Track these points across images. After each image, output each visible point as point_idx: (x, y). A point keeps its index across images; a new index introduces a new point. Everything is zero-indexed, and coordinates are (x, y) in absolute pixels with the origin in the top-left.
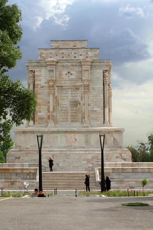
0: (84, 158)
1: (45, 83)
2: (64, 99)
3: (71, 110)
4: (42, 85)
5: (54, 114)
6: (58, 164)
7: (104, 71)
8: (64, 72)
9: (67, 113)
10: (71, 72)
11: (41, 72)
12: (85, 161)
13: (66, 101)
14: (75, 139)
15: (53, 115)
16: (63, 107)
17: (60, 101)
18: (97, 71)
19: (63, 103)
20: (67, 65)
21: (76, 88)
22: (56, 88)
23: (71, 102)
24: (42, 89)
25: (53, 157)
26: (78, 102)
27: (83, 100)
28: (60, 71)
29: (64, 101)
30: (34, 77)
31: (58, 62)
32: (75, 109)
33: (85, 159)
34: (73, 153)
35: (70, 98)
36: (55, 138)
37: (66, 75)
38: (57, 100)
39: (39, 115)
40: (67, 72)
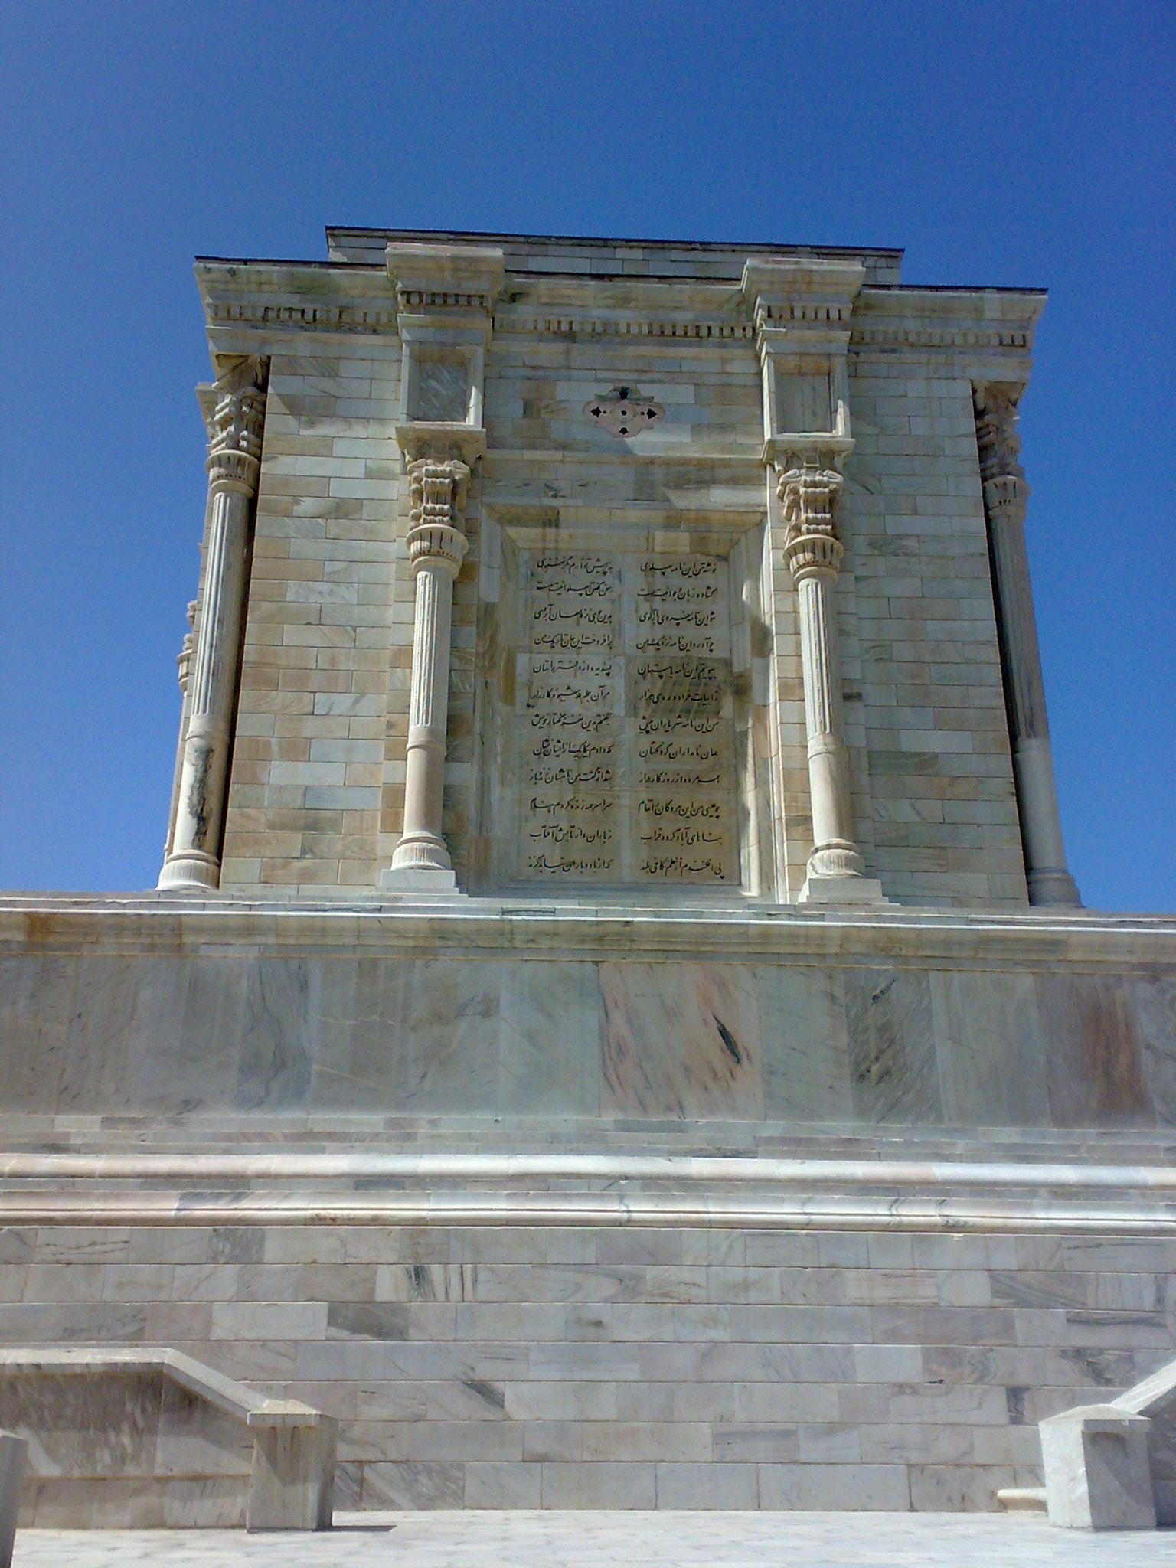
0: (882, 1294)
2: (570, 644)
3: (645, 742)
4: (336, 489)
5: (465, 774)
6: (484, 1391)
7: (980, 395)
8: (578, 393)
10: (645, 390)
11: (332, 374)
12: (894, 1336)
13: (593, 657)
14: (724, 1034)
15: (448, 790)
16: (561, 719)
18: (916, 387)
19: (557, 681)
20: (604, 334)
25: (419, 1274)
26: (720, 675)
28: (540, 373)
29: (567, 656)
30: (262, 427)
31: (514, 298)
32: (685, 739)
33: (894, 1308)
34: (715, 1210)
35: (635, 633)
36: (460, 1014)
37: (596, 412)
38: (493, 638)
39: (281, 789)
40: (606, 389)
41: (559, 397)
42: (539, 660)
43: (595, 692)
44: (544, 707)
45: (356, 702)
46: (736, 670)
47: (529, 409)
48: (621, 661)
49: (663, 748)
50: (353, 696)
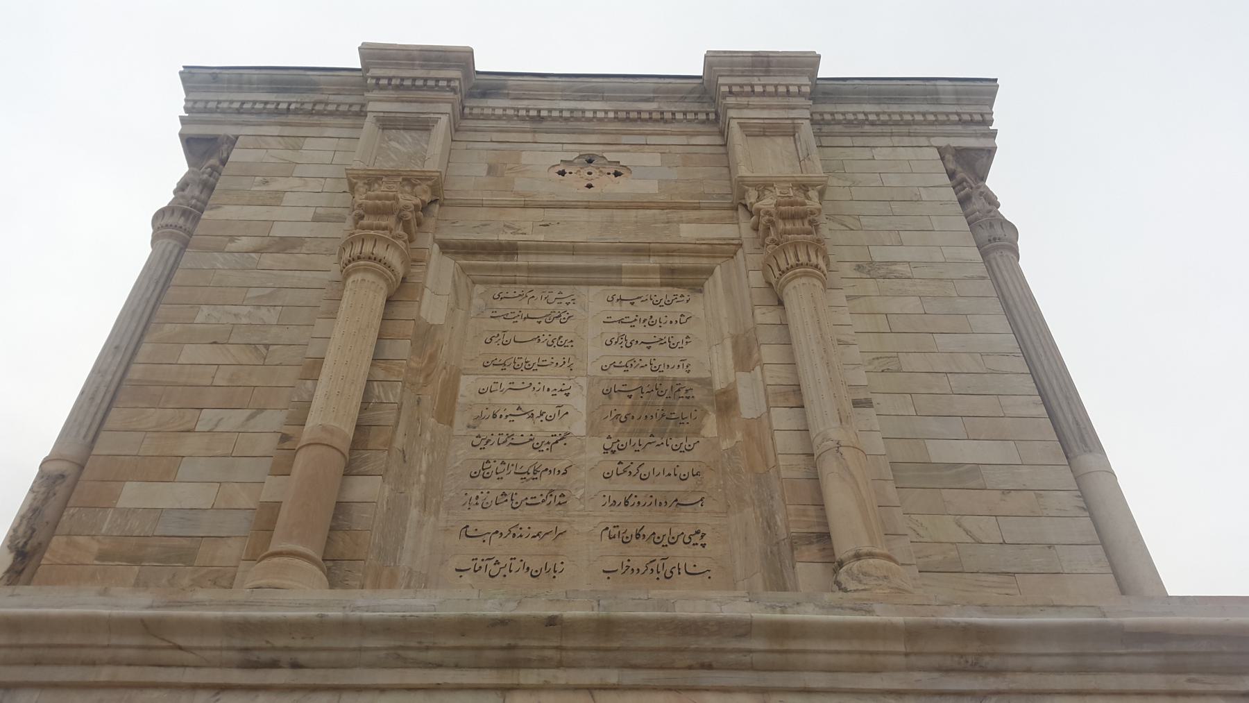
1: (317, 219)
3: (611, 463)
9: (558, 498)
10: (611, 157)
16: (510, 440)
17: (467, 386)
19: (510, 400)
21: (672, 277)
22: (440, 273)
23: (607, 393)
24: (267, 260)
27: (769, 353)
29: (519, 378)
32: (660, 458)
37: (562, 173)
38: (432, 358)
41: (523, 162)
42: (485, 383)
43: (550, 411)
44: (488, 426)
45: (252, 417)
46: (718, 386)
47: (491, 170)
48: (583, 382)
49: (633, 469)
50: (248, 412)
